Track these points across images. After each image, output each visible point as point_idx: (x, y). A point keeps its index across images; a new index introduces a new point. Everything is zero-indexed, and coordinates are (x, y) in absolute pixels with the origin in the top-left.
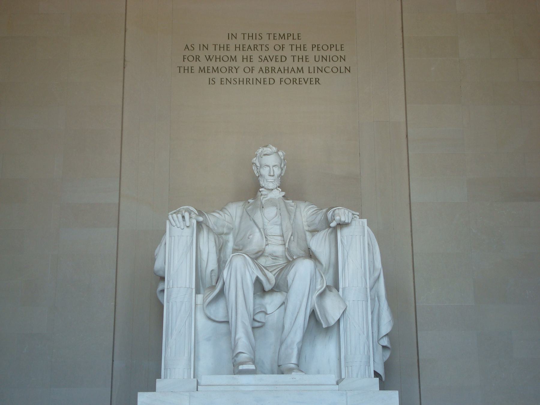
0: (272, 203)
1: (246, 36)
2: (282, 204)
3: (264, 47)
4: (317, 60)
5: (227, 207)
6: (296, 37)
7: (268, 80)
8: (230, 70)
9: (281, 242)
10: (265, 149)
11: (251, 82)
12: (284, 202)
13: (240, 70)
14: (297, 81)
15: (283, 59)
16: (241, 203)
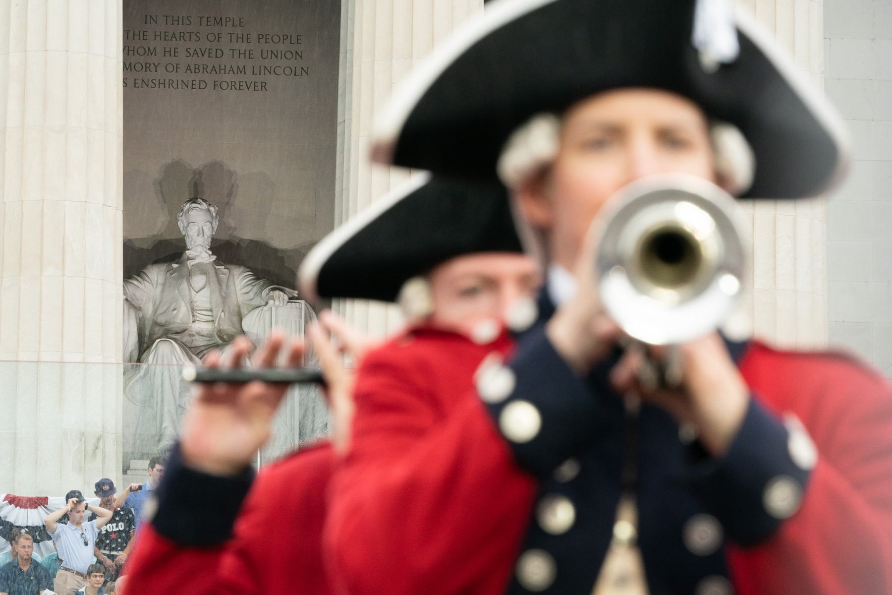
0: (201, 269)
1: (170, 20)
2: (212, 272)
3: (194, 37)
4: (265, 55)
5: (146, 271)
6: (237, 23)
7: (197, 83)
8: (147, 67)
9: (210, 318)
10: (194, 205)
11: (175, 84)
12: (215, 269)
13: (161, 69)
14: (237, 86)
15: (219, 53)
16: (163, 267)
